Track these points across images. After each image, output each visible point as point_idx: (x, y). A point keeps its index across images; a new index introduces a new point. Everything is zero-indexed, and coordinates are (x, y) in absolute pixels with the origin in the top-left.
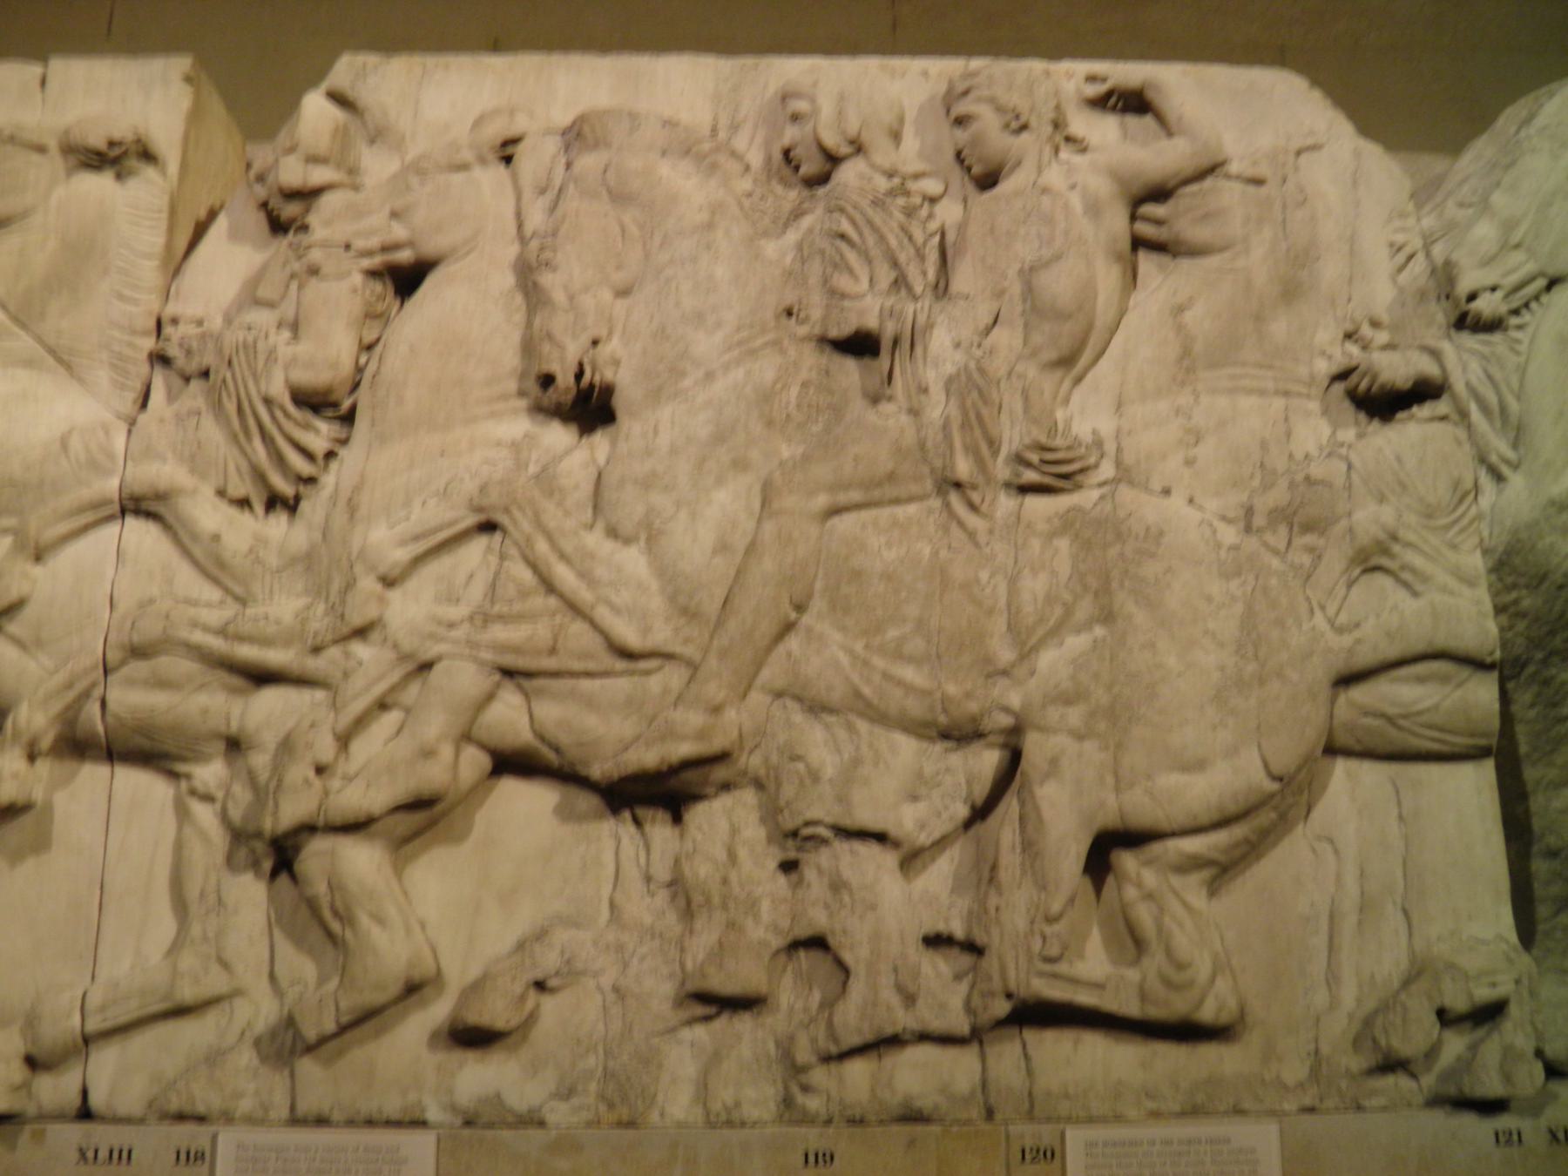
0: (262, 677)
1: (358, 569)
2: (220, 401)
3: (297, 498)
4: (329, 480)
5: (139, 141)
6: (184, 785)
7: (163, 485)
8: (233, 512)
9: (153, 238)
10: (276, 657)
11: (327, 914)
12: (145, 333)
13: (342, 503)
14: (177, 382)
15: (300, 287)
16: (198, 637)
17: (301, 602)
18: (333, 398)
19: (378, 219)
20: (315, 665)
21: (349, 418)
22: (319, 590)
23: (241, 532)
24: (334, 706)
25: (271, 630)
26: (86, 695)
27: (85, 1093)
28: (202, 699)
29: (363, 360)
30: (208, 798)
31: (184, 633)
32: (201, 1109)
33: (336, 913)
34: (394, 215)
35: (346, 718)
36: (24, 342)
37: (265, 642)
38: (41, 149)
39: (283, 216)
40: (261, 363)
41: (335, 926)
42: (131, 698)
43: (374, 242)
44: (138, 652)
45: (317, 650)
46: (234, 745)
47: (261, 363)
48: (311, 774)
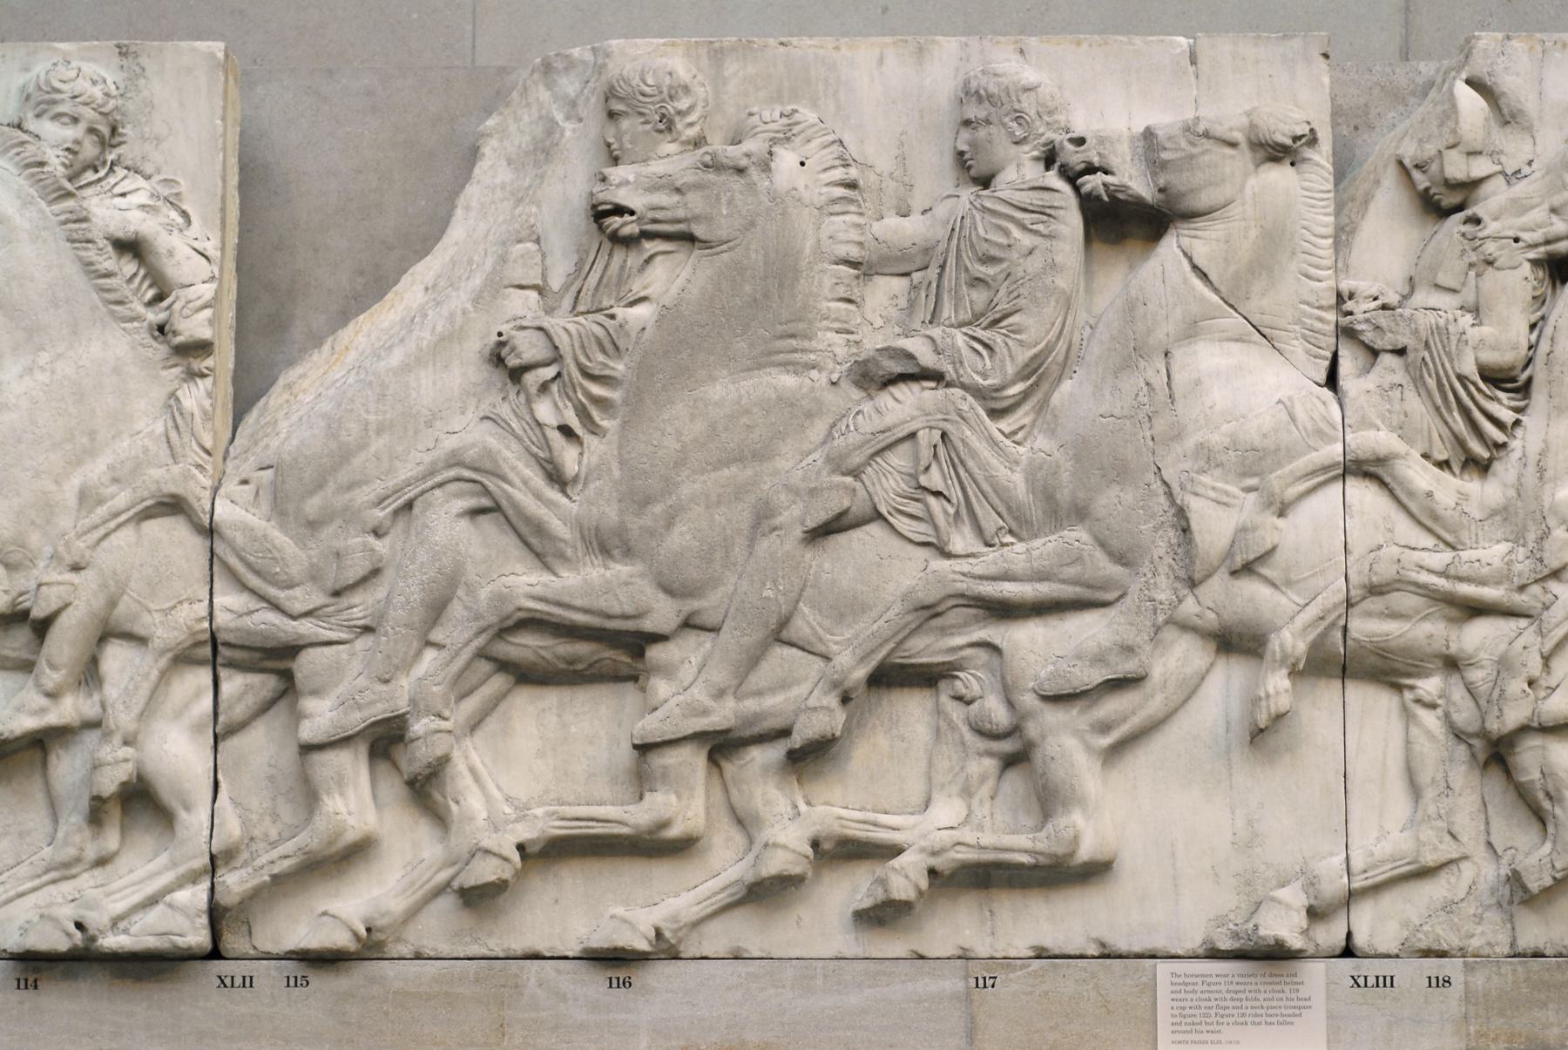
0: (1476, 610)
1: (1551, 522)
2: (1422, 377)
3: (1490, 461)
4: (1515, 444)
5: (1312, 130)
6: (1408, 695)
7: (1382, 452)
8: (1436, 470)
9: (1325, 221)
10: (1490, 593)
11: (1541, 795)
12: (1329, 308)
13: (1531, 469)
14: (1362, 356)
15: (1478, 275)
16: (1424, 578)
17: (1503, 547)
18: (1514, 373)
19: (1539, 214)
20: (1520, 599)
21: (1525, 390)
22: (1518, 539)
23: (1447, 489)
24: (1540, 633)
25: (1485, 570)
26: (1333, 624)
27: (1349, 935)
28: (1427, 627)
29: (1534, 337)
30: (1432, 706)
31: (1413, 576)
32: (1445, 947)
33: (1548, 794)
34: (1554, 210)
35: (1549, 646)
36: (1235, 322)
37: (1482, 582)
38: (1233, 145)
39: (1443, 201)
40: (1453, 347)
41: (1546, 804)
42: (1365, 627)
43: (1537, 236)
44: (1375, 590)
45: (1522, 588)
46: (1452, 664)
47: (1453, 347)
48: (1526, 686)
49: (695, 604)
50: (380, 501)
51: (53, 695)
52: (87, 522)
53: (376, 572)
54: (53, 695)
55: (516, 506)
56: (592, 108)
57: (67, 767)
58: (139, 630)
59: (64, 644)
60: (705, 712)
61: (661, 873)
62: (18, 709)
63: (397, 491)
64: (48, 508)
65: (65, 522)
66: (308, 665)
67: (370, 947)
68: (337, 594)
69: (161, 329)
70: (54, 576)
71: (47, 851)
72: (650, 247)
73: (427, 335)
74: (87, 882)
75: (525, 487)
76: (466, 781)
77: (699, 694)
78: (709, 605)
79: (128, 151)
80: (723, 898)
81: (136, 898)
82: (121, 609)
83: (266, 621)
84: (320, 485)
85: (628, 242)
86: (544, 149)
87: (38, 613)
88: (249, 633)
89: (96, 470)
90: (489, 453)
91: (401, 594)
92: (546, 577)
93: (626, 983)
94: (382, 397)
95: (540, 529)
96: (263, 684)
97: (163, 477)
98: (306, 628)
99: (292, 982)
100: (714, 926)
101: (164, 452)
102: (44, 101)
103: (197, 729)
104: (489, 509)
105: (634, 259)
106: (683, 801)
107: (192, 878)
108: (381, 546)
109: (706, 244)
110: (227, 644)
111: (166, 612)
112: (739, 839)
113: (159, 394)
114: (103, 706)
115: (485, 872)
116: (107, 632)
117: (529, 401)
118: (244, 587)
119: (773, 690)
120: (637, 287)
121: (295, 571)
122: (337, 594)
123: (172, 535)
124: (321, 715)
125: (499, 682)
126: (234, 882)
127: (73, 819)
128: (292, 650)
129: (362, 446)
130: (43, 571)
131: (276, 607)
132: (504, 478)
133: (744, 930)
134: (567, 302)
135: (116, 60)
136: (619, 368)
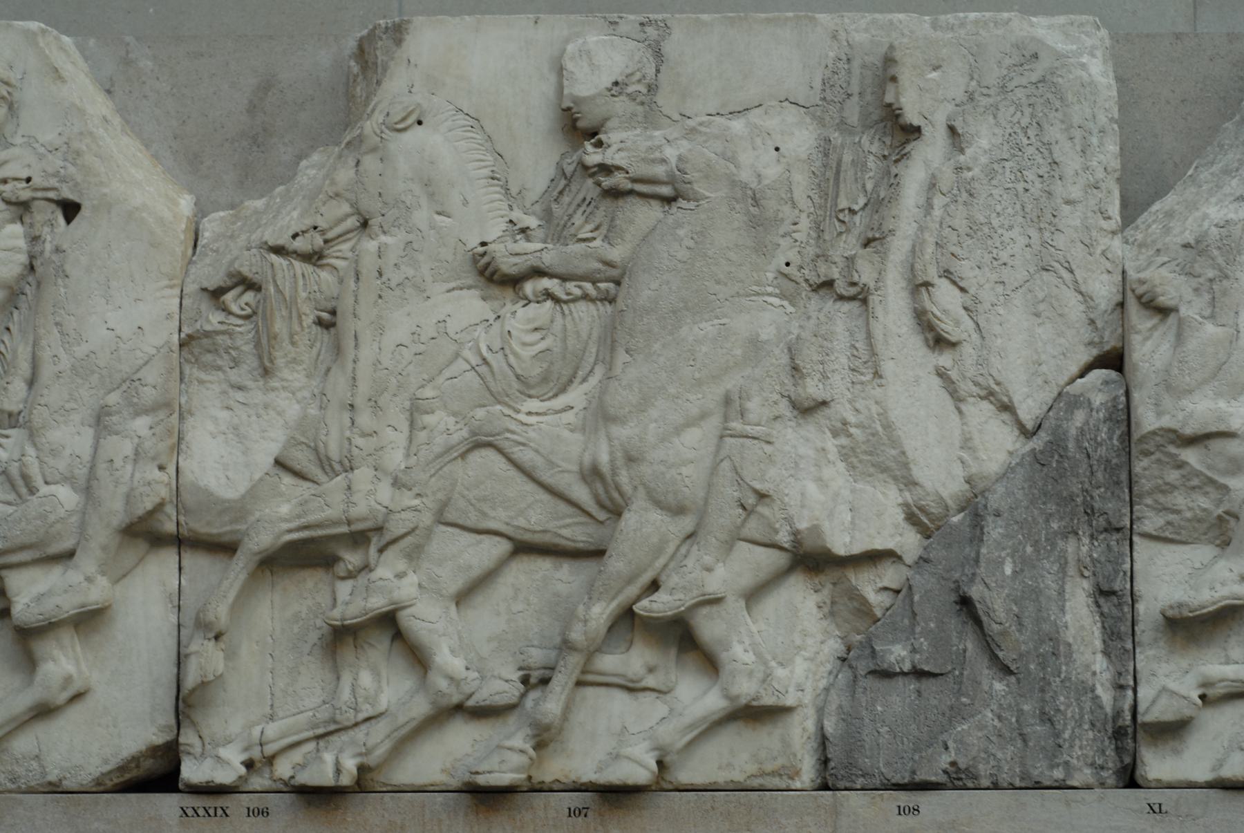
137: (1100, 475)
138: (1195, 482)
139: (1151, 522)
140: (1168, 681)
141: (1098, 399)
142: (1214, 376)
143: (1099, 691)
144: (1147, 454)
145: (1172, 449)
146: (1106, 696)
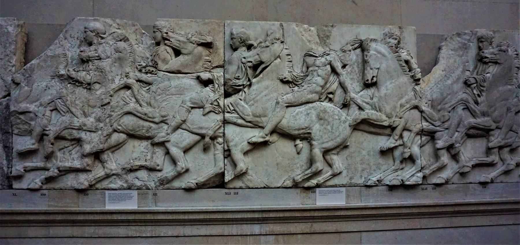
49: (498, 124)
50: (450, 107)
51: (396, 140)
52: (403, 110)
53: (449, 119)
54: (396, 140)
55: (471, 108)
56: (475, 41)
57: (397, 153)
58: (410, 129)
59: (398, 131)
60: (500, 142)
61: (490, 169)
62: (391, 143)
63: (453, 105)
64: (395, 107)
65: (398, 110)
66: (438, 135)
67: (447, 182)
68: (443, 123)
69: (413, 76)
70: (397, 119)
71: (393, 167)
72: (490, 64)
73: (454, 78)
74: (399, 172)
75: (472, 105)
76: (461, 154)
77: (499, 139)
78: (501, 124)
79: (401, 45)
80: (501, 173)
81: (410, 175)
82: (407, 125)
83: (431, 127)
84: (440, 104)
85: (486, 63)
86: (465, 47)
87: (394, 126)
88: (429, 129)
89: (403, 101)
90: (467, 99)
91: (454, 122)
92: (474, 120)
93: (485, 187)
94: (449, 89)
95: (475, 112)
96: (429, 138)
97: (415, 102)
98: (438, 128)
99: (433, 189)
100: (498, 178)
101: (414, 98)
102: (391, 36)
103: (418, 146)
104: (467, 108)
105: (487, 66)
106: (494, 158)
107: (417, 172)
108: (450, 114)
109: (499, 63)
110: (425, 131)
111: (415, 126)
112: (501, 163)
113: (411, 88)
114: (403, 142)
115: (467, 170)
116: (405, 129)
117: (472, 90)
118: (427, 121)
119: (509, 139)
120: (487, 71)
121: (437, 119)
122: (443, 123)
123: (416, 113)
124: (440, 144)
125: (466, 137)
126: (427, 172)
127: (398, 162)
128: (435, 132)
129: (446, 97)
130: (394, 119)
131: (433, 125)
132: (469, 103)
133: (502, 178)
134: (475, 73)
135: (399, 29)
136: (485, 84)
137: (3, 121)
138: (23, 122)
139: (16, 131)
140: (18, 167)
141: (4, 103)
142: (26, 99)
143: (4, 168)
144: (13, 116)
145: (17, 115)
146: (5, 169)
